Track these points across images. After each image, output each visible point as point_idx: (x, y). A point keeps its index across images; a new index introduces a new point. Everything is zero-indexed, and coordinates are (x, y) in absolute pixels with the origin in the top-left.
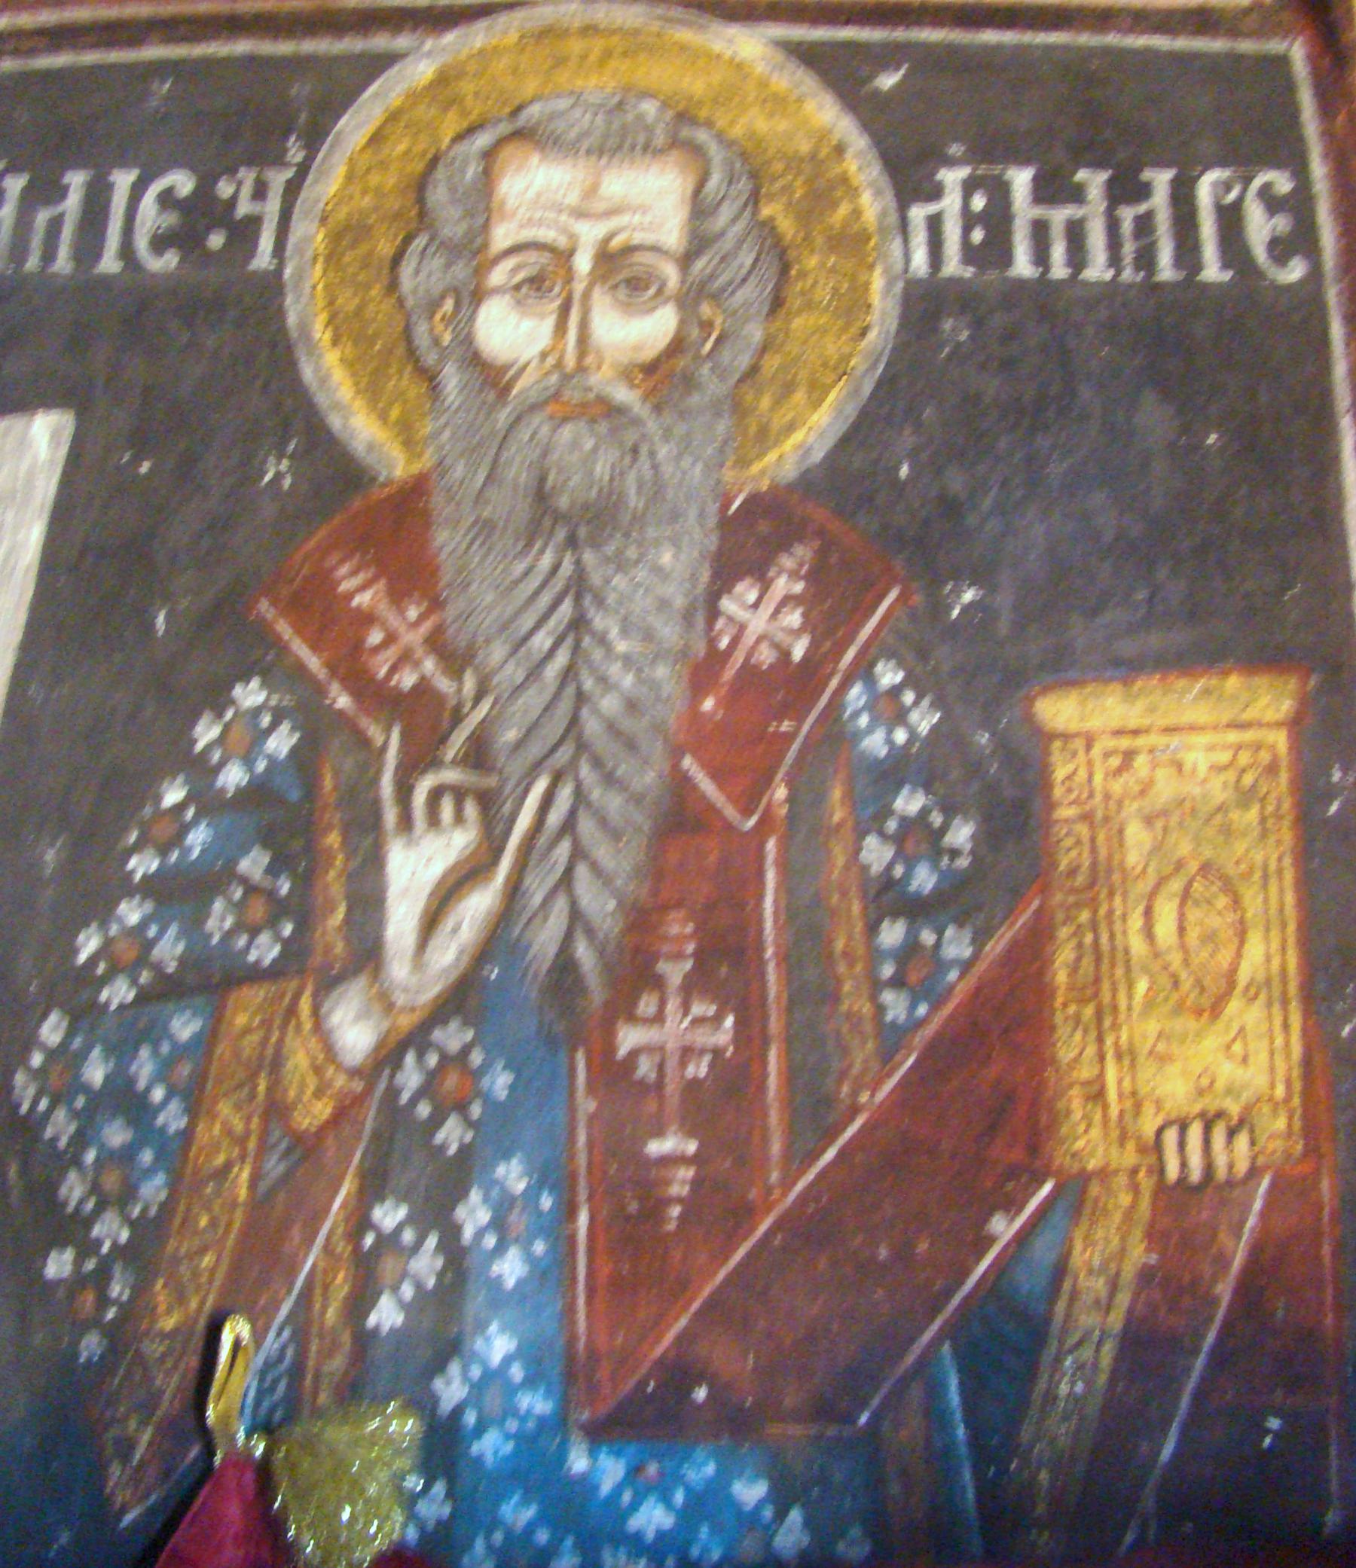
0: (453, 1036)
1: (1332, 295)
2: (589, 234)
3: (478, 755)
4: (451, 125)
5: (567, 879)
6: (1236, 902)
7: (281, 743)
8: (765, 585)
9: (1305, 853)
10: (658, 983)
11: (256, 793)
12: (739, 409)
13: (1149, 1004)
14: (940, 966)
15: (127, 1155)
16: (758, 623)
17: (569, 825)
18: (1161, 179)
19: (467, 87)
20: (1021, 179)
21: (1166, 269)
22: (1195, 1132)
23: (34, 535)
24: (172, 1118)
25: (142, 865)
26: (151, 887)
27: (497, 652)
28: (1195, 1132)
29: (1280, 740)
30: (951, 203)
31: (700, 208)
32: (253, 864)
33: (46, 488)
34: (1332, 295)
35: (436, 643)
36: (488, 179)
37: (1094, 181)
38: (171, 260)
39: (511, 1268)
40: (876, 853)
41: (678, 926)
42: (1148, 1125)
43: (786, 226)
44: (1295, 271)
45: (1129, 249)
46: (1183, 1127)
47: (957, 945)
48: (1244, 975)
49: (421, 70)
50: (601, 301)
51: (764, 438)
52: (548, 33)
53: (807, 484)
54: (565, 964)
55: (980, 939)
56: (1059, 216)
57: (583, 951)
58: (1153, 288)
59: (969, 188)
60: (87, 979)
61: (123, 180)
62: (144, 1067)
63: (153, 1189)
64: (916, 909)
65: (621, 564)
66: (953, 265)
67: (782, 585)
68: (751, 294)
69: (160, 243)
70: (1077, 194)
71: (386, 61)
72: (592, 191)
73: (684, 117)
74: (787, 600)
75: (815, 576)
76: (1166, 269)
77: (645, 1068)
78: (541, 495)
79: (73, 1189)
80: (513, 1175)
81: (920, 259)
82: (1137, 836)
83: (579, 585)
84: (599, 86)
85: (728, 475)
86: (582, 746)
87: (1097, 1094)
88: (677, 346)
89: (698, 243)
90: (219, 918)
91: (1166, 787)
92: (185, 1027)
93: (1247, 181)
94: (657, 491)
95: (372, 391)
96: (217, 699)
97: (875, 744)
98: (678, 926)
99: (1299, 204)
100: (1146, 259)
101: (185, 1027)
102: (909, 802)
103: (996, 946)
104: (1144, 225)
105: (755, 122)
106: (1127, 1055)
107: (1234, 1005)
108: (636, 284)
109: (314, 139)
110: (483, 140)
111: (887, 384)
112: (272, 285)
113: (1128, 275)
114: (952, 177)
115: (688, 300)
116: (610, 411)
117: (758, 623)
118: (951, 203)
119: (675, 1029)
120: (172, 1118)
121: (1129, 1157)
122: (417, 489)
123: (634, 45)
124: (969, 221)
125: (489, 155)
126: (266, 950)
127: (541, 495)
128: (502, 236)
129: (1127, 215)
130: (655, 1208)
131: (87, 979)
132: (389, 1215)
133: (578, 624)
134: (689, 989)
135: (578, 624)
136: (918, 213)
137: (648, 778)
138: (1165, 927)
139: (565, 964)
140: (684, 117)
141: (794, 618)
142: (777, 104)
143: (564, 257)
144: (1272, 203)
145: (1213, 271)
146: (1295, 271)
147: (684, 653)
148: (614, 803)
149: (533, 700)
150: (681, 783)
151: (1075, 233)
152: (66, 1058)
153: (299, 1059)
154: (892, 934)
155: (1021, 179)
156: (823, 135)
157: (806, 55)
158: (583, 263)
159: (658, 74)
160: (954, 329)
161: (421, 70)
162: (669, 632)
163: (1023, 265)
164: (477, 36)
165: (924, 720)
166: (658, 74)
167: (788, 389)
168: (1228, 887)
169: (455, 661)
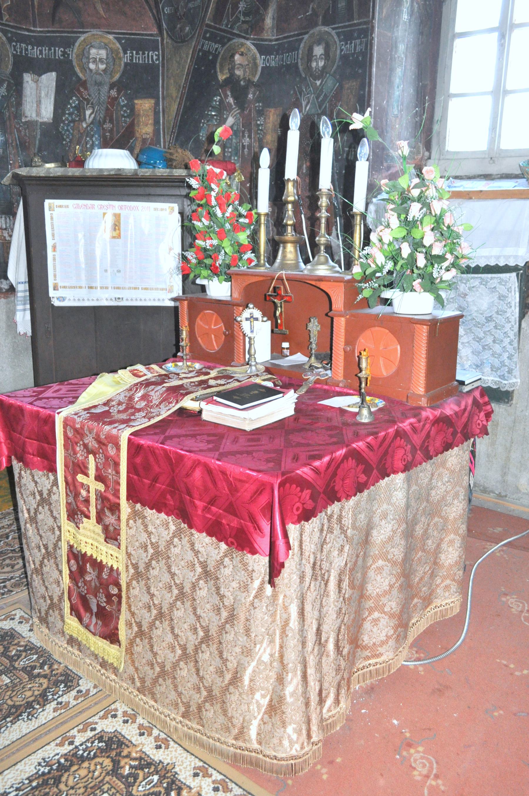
0: (92, 126)
2: (98, 57)
3: (92, 104)
7: (77, 102)
11: (75, 107)
15: (68, 135)
18: (146, 52)
20: (134, 52)
23: (55, 83)
24: (72, 132)
25: (67, 112)
26: (68, 114)
30: (128, 55)
31: (107, 55)
32: (76, 112)
33: (55, 79)
35: (88, 94)
37: (141, 53)
38: (62, 58)
39: (97, 143)
40: (122, 113)
41: (108, 118)
44: (157, 62)
47: (128, 120)
49: (82, 38)
51: (113, 77)
52: (93, 35)
54: (100, 121)
56: (138, 56)
60: (64, 121)
61: (57, 49)
62: (69, 128)
63: (71, 137)
64: (125, 117)
68: (112, 64)
69: (61, 56)
71: (79, 37)
73: (106, 45)
75: (117, 90)
79: (65, 137)
80: (97, 136)
83: (99, 90)
84: (98, 41)
88: (106, 68)
89: (107, 58)
90: (74, 116)
91: (144, 108)
92: (72, 125)
95: (81, 72)
96: (72, 99)
98: (108, 118)
99: (159, 55)
101: (72, 125)
102: (125, 109)
105: (111, 46)
109: (74, 45)
111: (123, 72)
112: (71, 61)
118: (128, 55)
119: (108, 126)
120: (72, 132)
122: (85, 81)
123: (101, 37)
126: (77, 119)
128: (91, 57)
130: (107, 138)
131: (64, 121)
132: (88, 139)
133: (99, 93)
137: (105, 106)
139: (100, 121)
140: (106, 45)
142: (114, 43)
143: (96, 59)
144: (156, 55)
145: (150, 62)
146: (157, 62)
149: (96, 100)
151: (139, 58)
152: (63, 127)
153: (81, 127)
155: (134, 52)
157: (115, 38)
159: (103, 40)
160: (129, 67)
161: (82, 38)
163: (134, 61)
166: (103, 40)
169: (90, 95)
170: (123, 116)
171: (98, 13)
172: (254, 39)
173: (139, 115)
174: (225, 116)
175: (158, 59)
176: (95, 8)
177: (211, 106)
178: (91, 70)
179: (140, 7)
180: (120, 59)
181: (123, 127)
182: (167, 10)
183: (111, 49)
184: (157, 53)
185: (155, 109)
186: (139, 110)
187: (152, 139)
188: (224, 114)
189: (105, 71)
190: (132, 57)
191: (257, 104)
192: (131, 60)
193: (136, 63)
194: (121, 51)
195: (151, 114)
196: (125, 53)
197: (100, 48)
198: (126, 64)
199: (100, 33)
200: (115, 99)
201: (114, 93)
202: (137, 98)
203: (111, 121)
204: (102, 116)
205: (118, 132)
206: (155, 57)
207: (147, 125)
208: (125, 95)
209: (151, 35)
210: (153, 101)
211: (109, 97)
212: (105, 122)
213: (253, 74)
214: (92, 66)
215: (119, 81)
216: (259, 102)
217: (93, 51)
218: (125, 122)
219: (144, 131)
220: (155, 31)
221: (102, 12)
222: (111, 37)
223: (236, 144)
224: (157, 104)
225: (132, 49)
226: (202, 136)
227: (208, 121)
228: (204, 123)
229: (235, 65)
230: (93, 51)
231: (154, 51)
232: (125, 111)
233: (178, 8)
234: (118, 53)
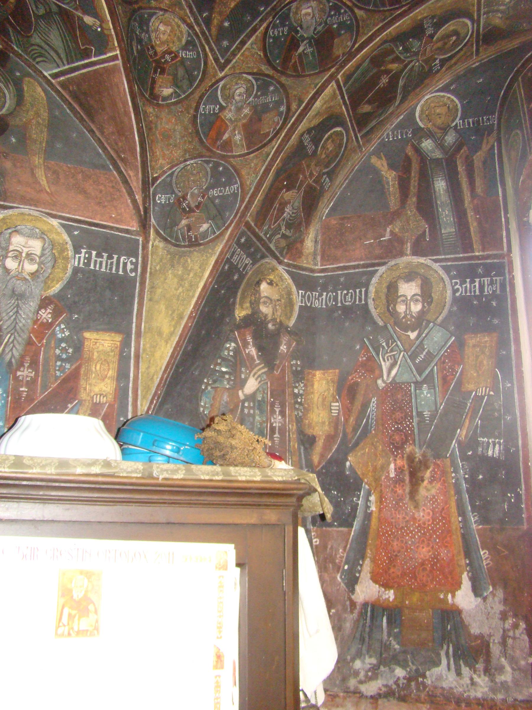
1: (138, 279)
2: (25, 250)
4: (5, 227)
5: (12, 349)
6: (109, 366)
8: (46, 310)
9: (119, 360)
10: (24, 366)
12: (46, 283)
13: (94, 378)
14: (65, 368)
16: (44, 316)
17: (13, 342)
18: (116, 257)
19: (8, 221)
20: (94, 253)
21: (114, 271)
22: (99, 396)
27: (4, 314)
28: (99, 396)
29: (118, 343)
30: (82, 255)
31: (43, 249)
34: (138, 279)
36: (10, 237)
37: (105, 255)
40: (58, 352)
41: (28, 358)
42: (92, 394)
43: (56, 254)
44: (133, 274)
45: (109, 267)
46: (97, 395)
47: (68, 366)
48: (108, 375)
50: (26, 261)
51: (49, 288)
52: (22, 214)
53: (54, 296)
54: (10, 362)
55: (71, 366)
56: (99, 260)
57: (13, 360)
58: (111, 273)
59: (86, 253)
64: (63, 360)
65: (24, 304)
66: (81, 265)
67: (49, 311)
68: (50, 265)
70: (102, 257)
72: (26, 243)
73: (43, 233)
74: (50, 313)
75: (54, 310)
76: (114, 271)
77: (21, 378)
78: (13, 291)
81: (76, 263)
82: (96, 354)
83: (18, 306)
84: (29, 225)
85: (42, 293)
86: (16, 330)
87: (85, 389)
88: (37, 271)
89: (43, 255)
91: (101, 348)
93: (128, 259)
94: (31, 293)
97: (59, 336)
98: (28, 358)
99: (136, 264)
100: (111, 269)
102: (63, 345)
103: (73, 367)
104: (112, 263)
105: (54, 236)
106: (90, 385)
107: (106, 380)
108: (32, 260)
110: (10, 231)
111: (68, 283)
113: (108, 271)
114: (83, 251)
115: (39, 264)
116: (25, 279)
117: (44, 316)
118: (82, 255)
119: (26, 373)
121: (89, 398)
123: (36, 218)
124: (85, 258)
125: (10, 234)
127: (13, 291)
128: (11, 248)
129: (109, 261)
130: (20, 398)
133: (17, 312)
134: (29, 367)
135: (17, 312)
136: (77, 256)
137: (25, 336)
138: (98, 367)
139: (10, 362)
140: (43, 233)
141: (50, 316)
142: (58, 234)
143: (21, 253)
144: (132, 263)
145: (121, 272)
146: (133, 274)
147: (32, 319)
148: (20, 339)
149: (9, 323)
150: (30, 337)
151: (101, 263)
154: (59, 363)
156: (65, 240)
157: (63, 226)
158: (24, 255)
162: (31, 315)
163: (92, 267)
164: (10, 212)
165: (67, 333)
166: (39, 225)
167: (53, 281)
168: (108, 363)
170: (59, 358)
171: (37, 182)
172: (288, 265)
173: (90, 360)
174: (243, 376)
175: (135, 270)
176: (33, 174)
177: (220, 357)
178: (7, 271)
179: (113, 187)
180: (66, 259)
181: (57, 378)
182: (161, 199)
183: (53, 244)
184: (134, 260)
185: (121, 352)
186: (91, 352)
187: (111, 406)
188: (241, 372)
189: (34, 275)
190: (89, 259)
191: (294, 362)
192: (88, 264)
193: (95, 270)
194: (70, 246)
195: (114, 361)
196: (77, 251)
197: (31, 236)
198: (76, 270)
199: (36, 214)
200: (49, 326)
201: (46, 315)
202: (88, 329)
203: (34, 364)
204: (16, 354)
205: (45, 387)
206: (129, 267)
207: (103, 380)
208: (67, 322)
209: (127, 231)
210: (118, 338)
211: (35, 322)
212: (21, 364)
213: (286, 315)
214: (11, 264)
215: (60, 296)
216: (296, 360)
217: (17, 241)
218: (62, 369)
219: (96, 389)
220: (134, 226)
221: (44, 182)
222: (55, 222)
223: (261, 424)
224: (126, 344)
225: (90, 247)
226: (204, 407)
227: (215, 382)
228: (207, 384)
229: (260, 298)
230: (17, 241)
231: (129, 255)
232: (64, 350)
233: (184, 198)
234: (63, 250)
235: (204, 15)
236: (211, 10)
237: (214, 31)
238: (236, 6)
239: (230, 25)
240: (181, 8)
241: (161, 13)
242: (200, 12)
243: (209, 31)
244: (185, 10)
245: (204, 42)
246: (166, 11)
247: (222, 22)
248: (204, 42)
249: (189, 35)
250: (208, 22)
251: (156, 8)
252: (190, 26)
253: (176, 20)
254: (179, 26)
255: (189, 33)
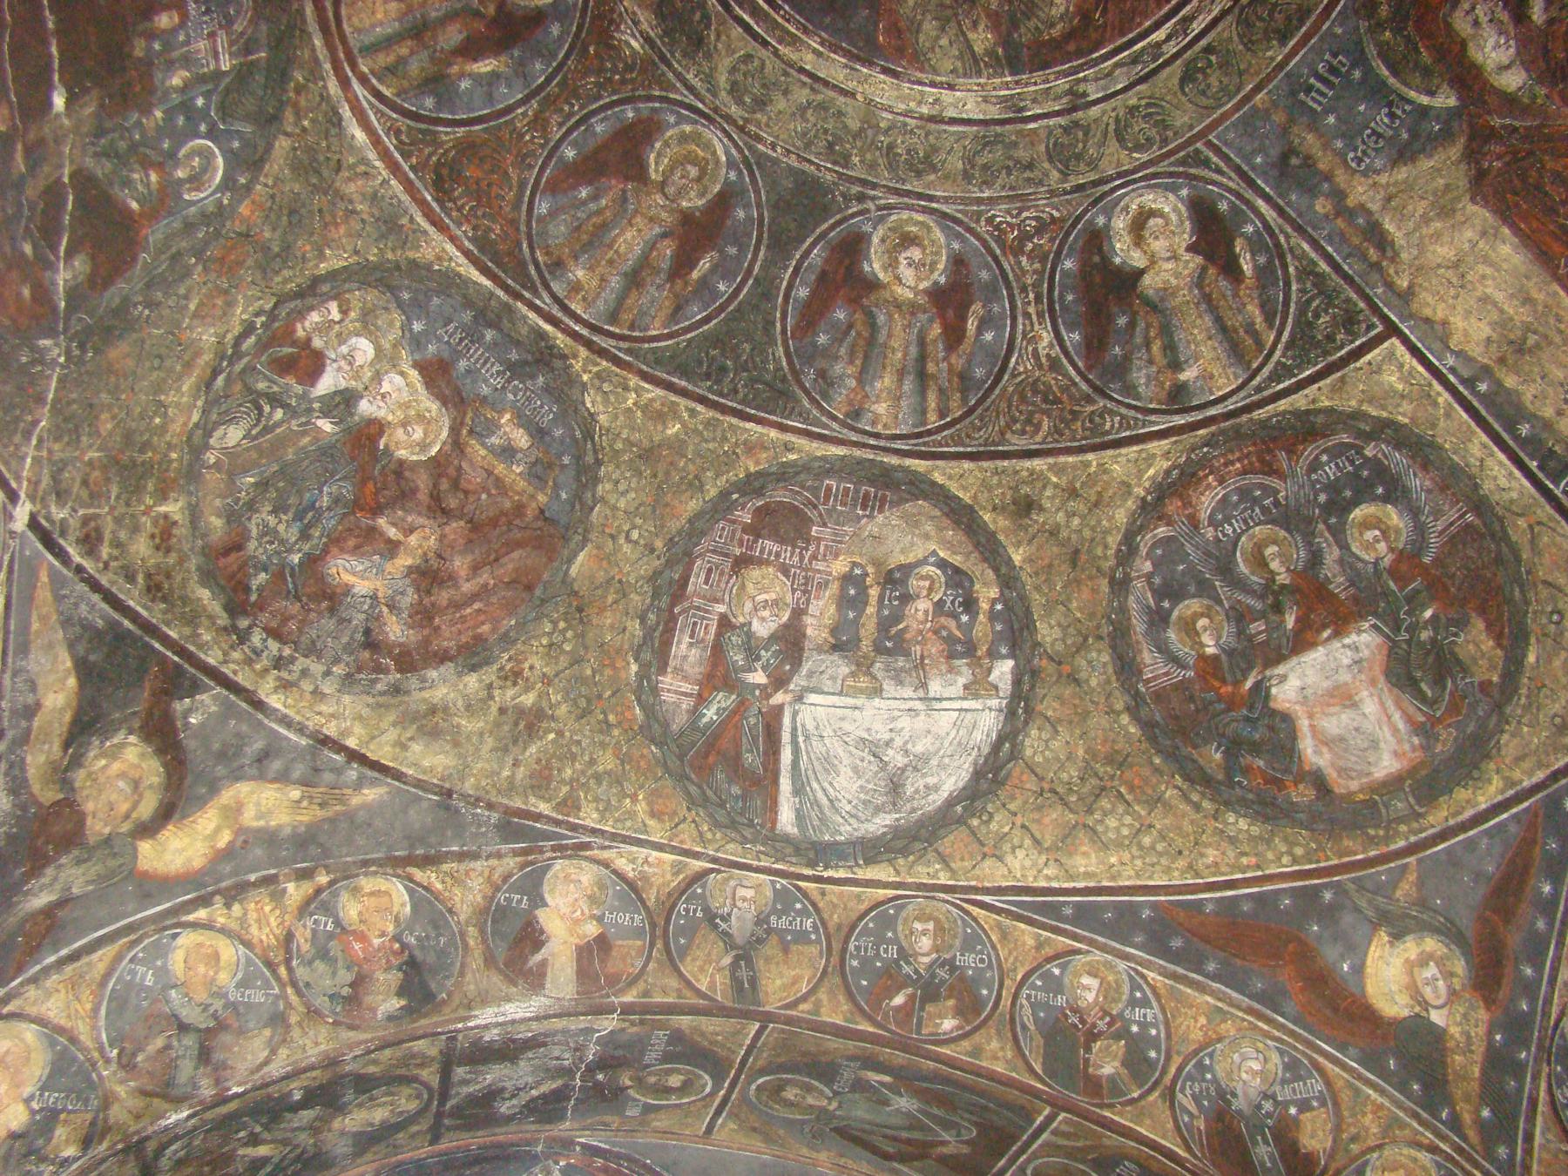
235: (1444, 1115)
236: (1449, 1101)
237: (1471, 1134)
238: (1483, 1072)
239: (1492, 1111)
240: (1403, 1126)
241: (1375, 1155)
242: (1435, 1114)
243: (1465, 1139)
244: (1409, 1125)
245: (1468, 1167)
246: (1380, 1147)
247: (1477, 1111)
248: (1468, 1167)
249: (1439, 1165)
250: (1455, 1123)
251: (1364, 1153)
252: (1433, 1149)
253: (1405, 1151)
254: (1415, 1160)
255: (1437, 1163)
